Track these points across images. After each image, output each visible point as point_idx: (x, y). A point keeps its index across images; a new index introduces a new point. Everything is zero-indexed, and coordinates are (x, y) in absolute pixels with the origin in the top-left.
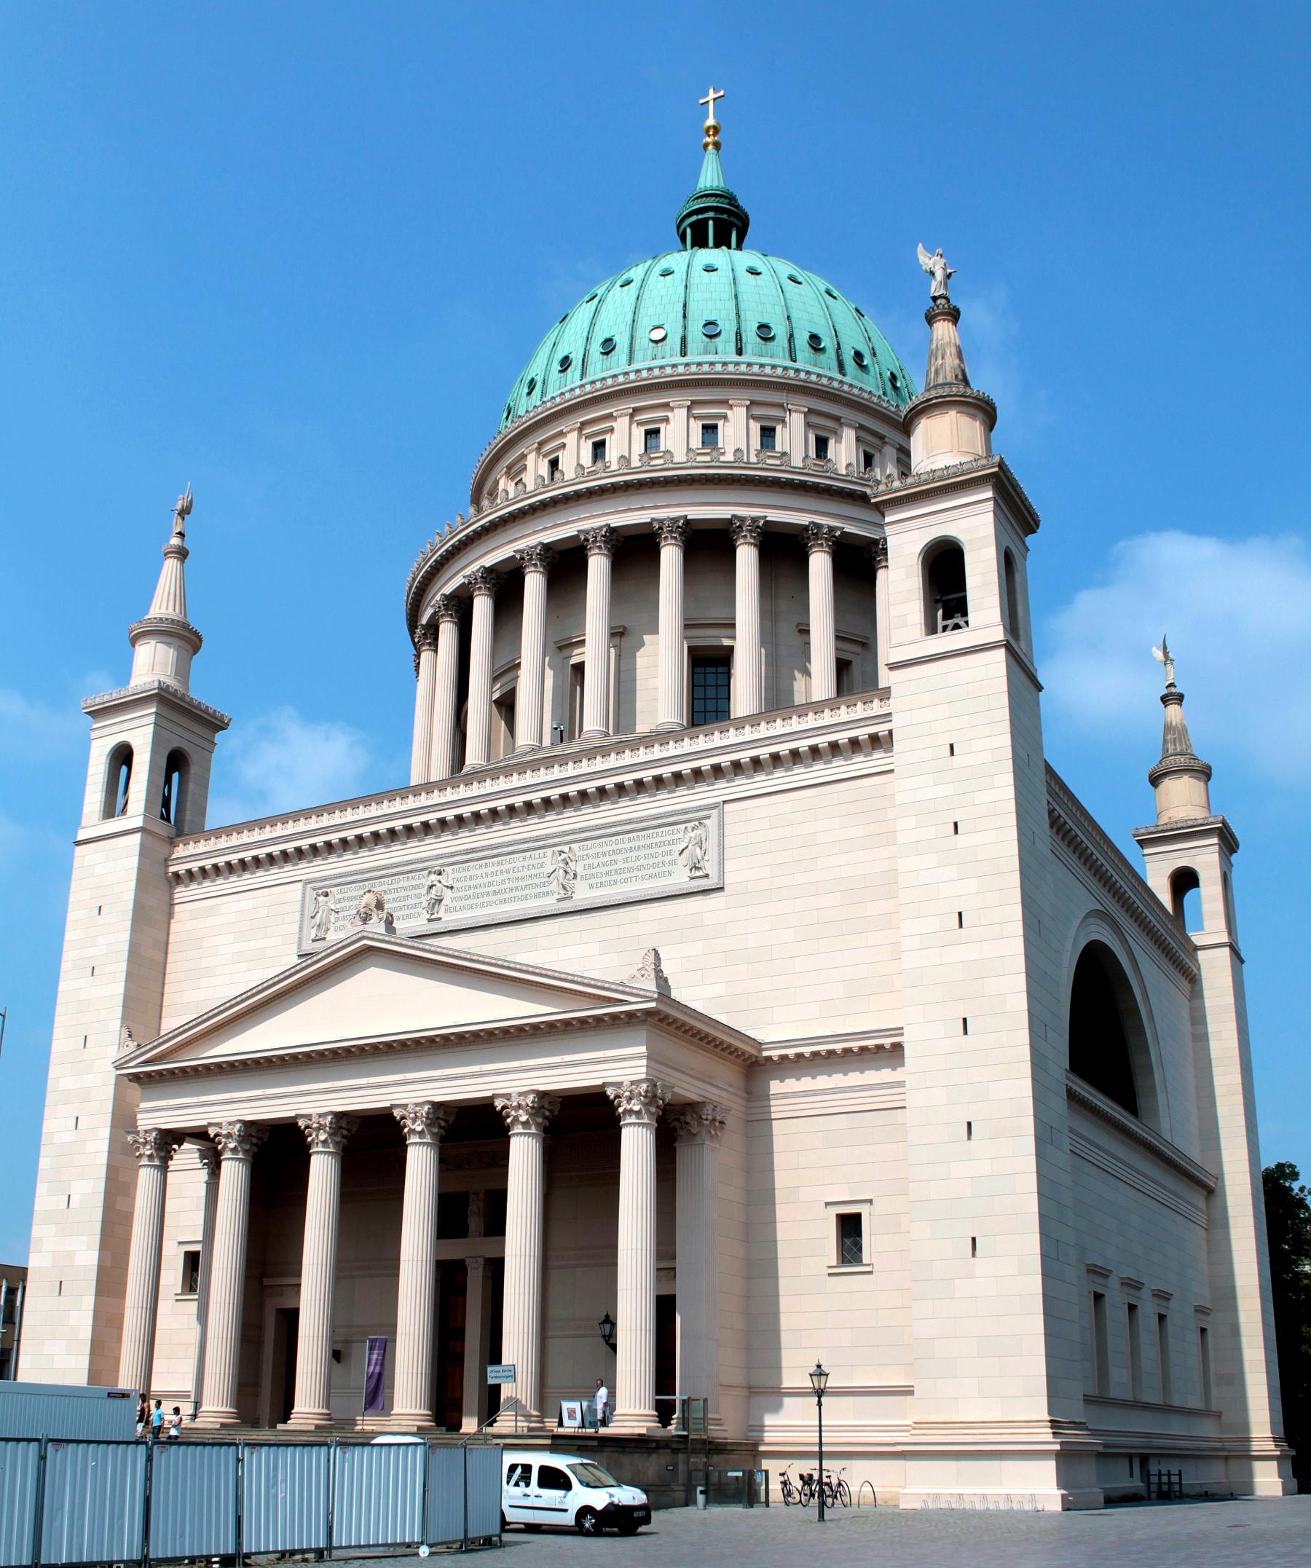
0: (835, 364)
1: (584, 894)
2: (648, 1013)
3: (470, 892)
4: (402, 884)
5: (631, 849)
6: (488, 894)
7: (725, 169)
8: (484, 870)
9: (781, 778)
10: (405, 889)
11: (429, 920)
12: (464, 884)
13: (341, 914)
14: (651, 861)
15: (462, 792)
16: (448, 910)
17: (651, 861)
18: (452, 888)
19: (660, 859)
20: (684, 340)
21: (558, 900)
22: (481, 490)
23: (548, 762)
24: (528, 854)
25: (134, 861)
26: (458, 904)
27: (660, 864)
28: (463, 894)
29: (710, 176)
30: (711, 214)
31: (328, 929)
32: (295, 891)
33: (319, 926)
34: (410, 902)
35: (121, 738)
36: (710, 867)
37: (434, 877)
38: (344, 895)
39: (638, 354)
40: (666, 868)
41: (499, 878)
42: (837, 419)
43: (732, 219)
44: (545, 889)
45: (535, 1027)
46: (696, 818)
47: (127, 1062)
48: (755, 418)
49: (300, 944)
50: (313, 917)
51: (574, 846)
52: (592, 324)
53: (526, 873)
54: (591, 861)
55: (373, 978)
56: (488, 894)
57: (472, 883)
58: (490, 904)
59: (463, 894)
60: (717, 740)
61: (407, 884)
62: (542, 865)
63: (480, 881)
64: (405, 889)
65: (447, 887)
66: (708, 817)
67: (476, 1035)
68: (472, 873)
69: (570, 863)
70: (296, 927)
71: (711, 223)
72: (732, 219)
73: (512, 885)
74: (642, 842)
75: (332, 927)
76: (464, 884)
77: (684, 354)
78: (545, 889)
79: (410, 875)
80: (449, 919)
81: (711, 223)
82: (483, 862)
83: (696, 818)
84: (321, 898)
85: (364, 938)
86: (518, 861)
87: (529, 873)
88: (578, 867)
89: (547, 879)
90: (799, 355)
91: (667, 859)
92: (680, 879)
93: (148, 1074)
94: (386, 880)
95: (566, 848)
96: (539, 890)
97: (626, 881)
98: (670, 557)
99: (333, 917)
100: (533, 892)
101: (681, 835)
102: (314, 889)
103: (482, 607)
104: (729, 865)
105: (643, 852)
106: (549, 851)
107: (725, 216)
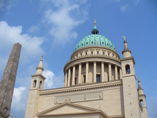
1: (87, 99)
2: (99, 112)
7: (97, 27)
8: (76, 96)
9: (109, 88)
15: (71, 88)
16: (72, 100)
22: (72, 57)
23: (82, 85)
29: (95, 28)
37: (70, 97)
42: (110, 52)
45: (85, 113)
46: (100, 92)
48: (102, 51)
52: (85, 41)
55: (66, 107)
60: (99, 84)
67: (79, 114)
70: (54, 101)
77: (95, 44)
80: (72, 101)
86: (80, 95)
88: (87, 96)
92: (98, 98)
93: (40, 116)
98: (95, 65)
103: (74, 69)
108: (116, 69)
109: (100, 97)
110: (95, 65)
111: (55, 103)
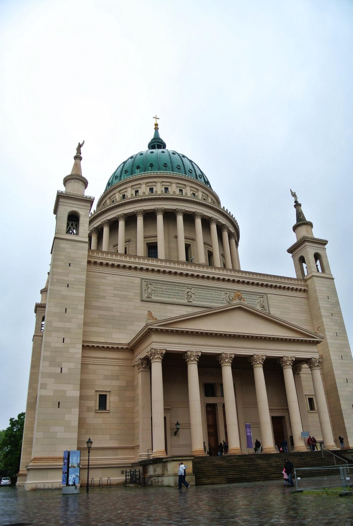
3: (200, 297)
4: (177, 288)
6: (206, 299)
8: (204, 292)
10: (178, 290)
11: (188, 301)
12: (197, 294)
13: (156, 292)
14: (251, 303)
16: (194, 300)
17: (251, 303)
18: (194, 294)
19: (252, 303)
24: (217, 291)
26: (197, 299)
27: (253, 304)
28: (198, 297)
30: (163, 145)
31: (152, 295)
32: (138, 281)
33: (149, 293)
34: (180, 294)
36: (266, 308)
38: (157, 286)
41: (209, 295)
44: (223, 302)
46: (262, 295)
47: (154, 324)
49: (141, 296)
50: (146, 290)
51: (230, 293)
53: (216, 296)
56: (206, 299)
57: (201, 294)
58: (206, 302)
59: (198, 297)
61: (179, 289)
62: (221, 295)
63: (202, 295)
64: (178, 290)
65: (193, 293)
66: (264, 296)
68: (200, 292)
69: (230, 297)
70: (139, 292)
73: (212, 298)
75: (153, 295)
76: (197, 294)
78: (223, 302)
79: (180, 287)
82: (203, 290)
83: (262, 295)
84: (149, 285)
85: (241, 304)
87: (218, 296)
89: (223, 299)
91: (255, 303)
94: (171, 286)
95: (228, 293)
96: (221, 302)
99: (153, 292)
100: (218, 301)
101: (257, 298)
102: (145, 282)
104: (271, 309)
105: (248, 300)
106: (223, 293)
109: (264, 308)
111: (144, 298)
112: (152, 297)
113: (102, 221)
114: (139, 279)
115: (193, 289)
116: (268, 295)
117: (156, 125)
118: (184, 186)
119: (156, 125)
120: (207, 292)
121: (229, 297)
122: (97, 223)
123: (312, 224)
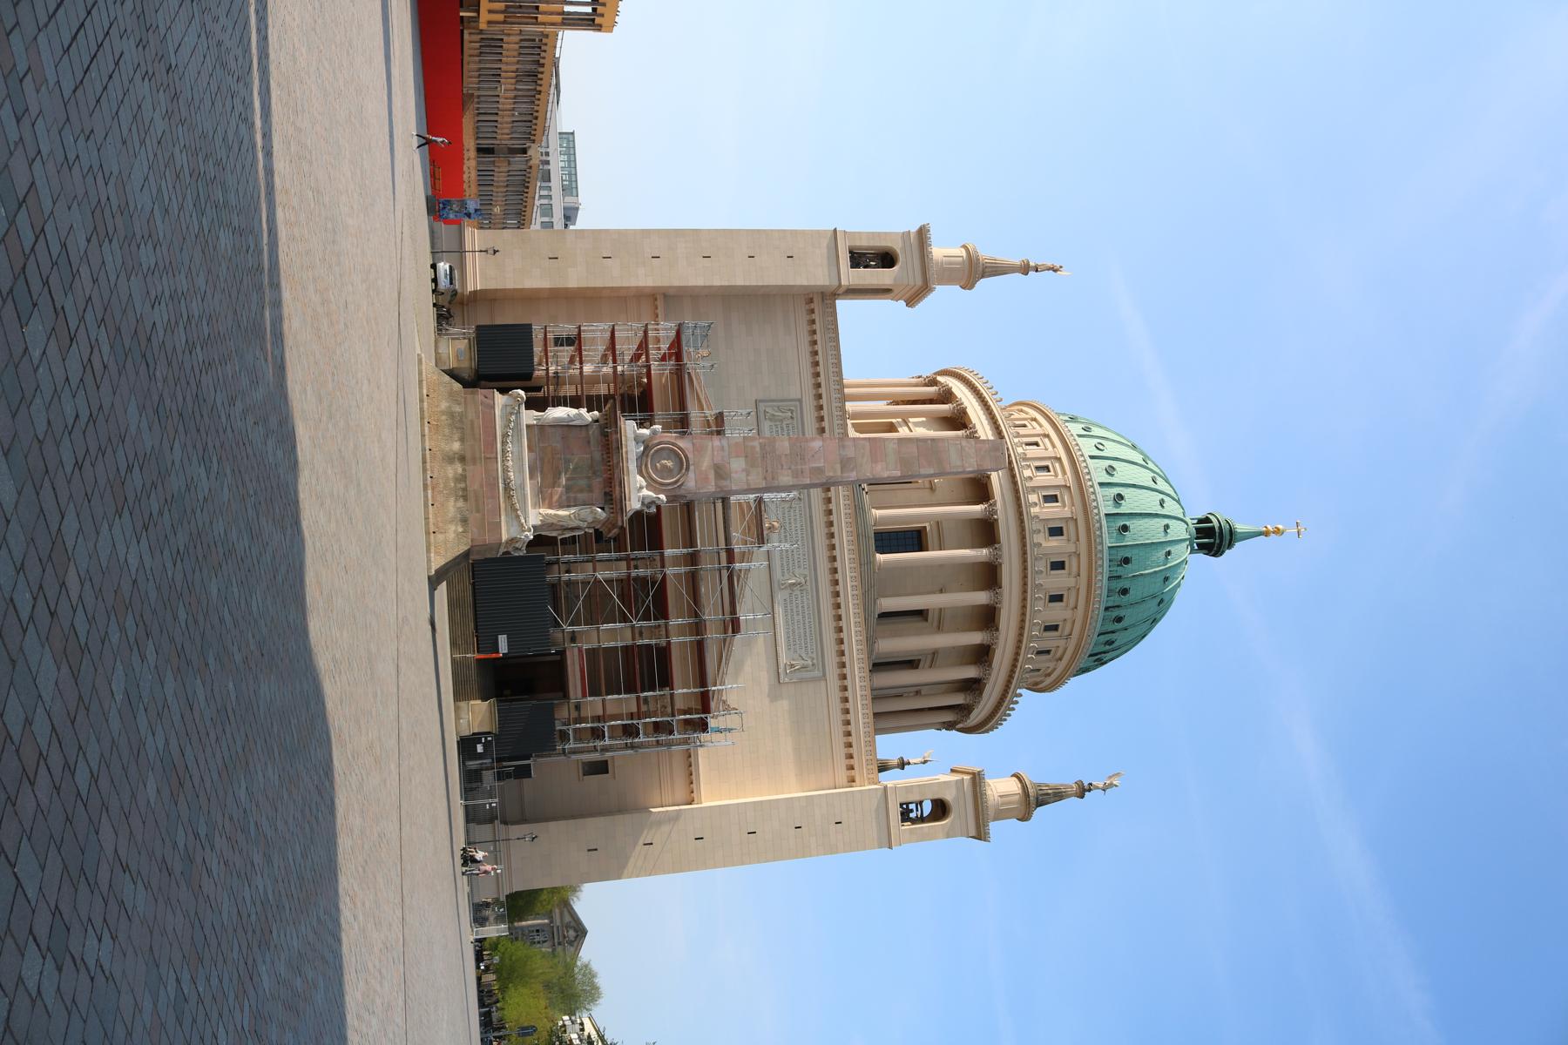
0: (1095, 652)
5: (804, 623)
20: (1119, 577)
21: (779, 581)
24: (806, 557)
25: (819, 283)
30: (1218, 541)
31: (770, 420)
35: (901, 258)
39: (1114, 551)
40: (792, 647)
42: (1060, 659)
43: (1212, 553)
49: (761, 401)
50: (778, 407)
51: (809, 589)
54: (799, 599)
57: (792, 521)
70: (773, 397)
71: (1212, 540)
72: (1212, 553)
74: (808, 630)
78: (785, 571)
81: (1212, 540)
90: (1102, 637)
97: (787, 622)
102: (796, 407)
105: (802, 631)
106: (807, 572)
107: (1215, 548)
108: (958, 699)
110: (981, 598)
111: (762, 406)
112: (768, 421)
113: (948, 382)
114: (799, 397)
115: (802, 505)
116: (823, 683)
117: (1278, 532)
118: (1073, 537)
119: (1278, 532)
120: (800, 536)
121: (799, 584)
122: (939, 378)
123: (983, 732)
